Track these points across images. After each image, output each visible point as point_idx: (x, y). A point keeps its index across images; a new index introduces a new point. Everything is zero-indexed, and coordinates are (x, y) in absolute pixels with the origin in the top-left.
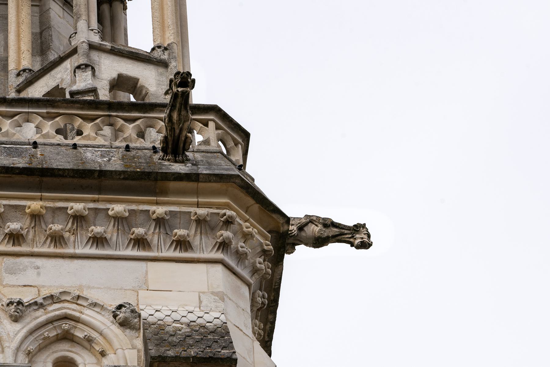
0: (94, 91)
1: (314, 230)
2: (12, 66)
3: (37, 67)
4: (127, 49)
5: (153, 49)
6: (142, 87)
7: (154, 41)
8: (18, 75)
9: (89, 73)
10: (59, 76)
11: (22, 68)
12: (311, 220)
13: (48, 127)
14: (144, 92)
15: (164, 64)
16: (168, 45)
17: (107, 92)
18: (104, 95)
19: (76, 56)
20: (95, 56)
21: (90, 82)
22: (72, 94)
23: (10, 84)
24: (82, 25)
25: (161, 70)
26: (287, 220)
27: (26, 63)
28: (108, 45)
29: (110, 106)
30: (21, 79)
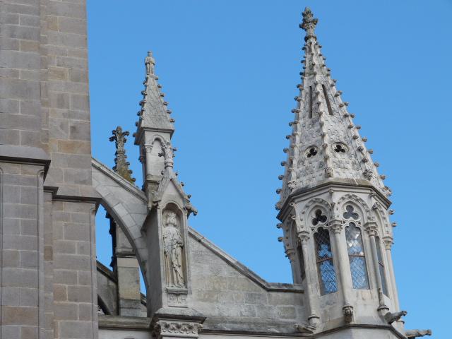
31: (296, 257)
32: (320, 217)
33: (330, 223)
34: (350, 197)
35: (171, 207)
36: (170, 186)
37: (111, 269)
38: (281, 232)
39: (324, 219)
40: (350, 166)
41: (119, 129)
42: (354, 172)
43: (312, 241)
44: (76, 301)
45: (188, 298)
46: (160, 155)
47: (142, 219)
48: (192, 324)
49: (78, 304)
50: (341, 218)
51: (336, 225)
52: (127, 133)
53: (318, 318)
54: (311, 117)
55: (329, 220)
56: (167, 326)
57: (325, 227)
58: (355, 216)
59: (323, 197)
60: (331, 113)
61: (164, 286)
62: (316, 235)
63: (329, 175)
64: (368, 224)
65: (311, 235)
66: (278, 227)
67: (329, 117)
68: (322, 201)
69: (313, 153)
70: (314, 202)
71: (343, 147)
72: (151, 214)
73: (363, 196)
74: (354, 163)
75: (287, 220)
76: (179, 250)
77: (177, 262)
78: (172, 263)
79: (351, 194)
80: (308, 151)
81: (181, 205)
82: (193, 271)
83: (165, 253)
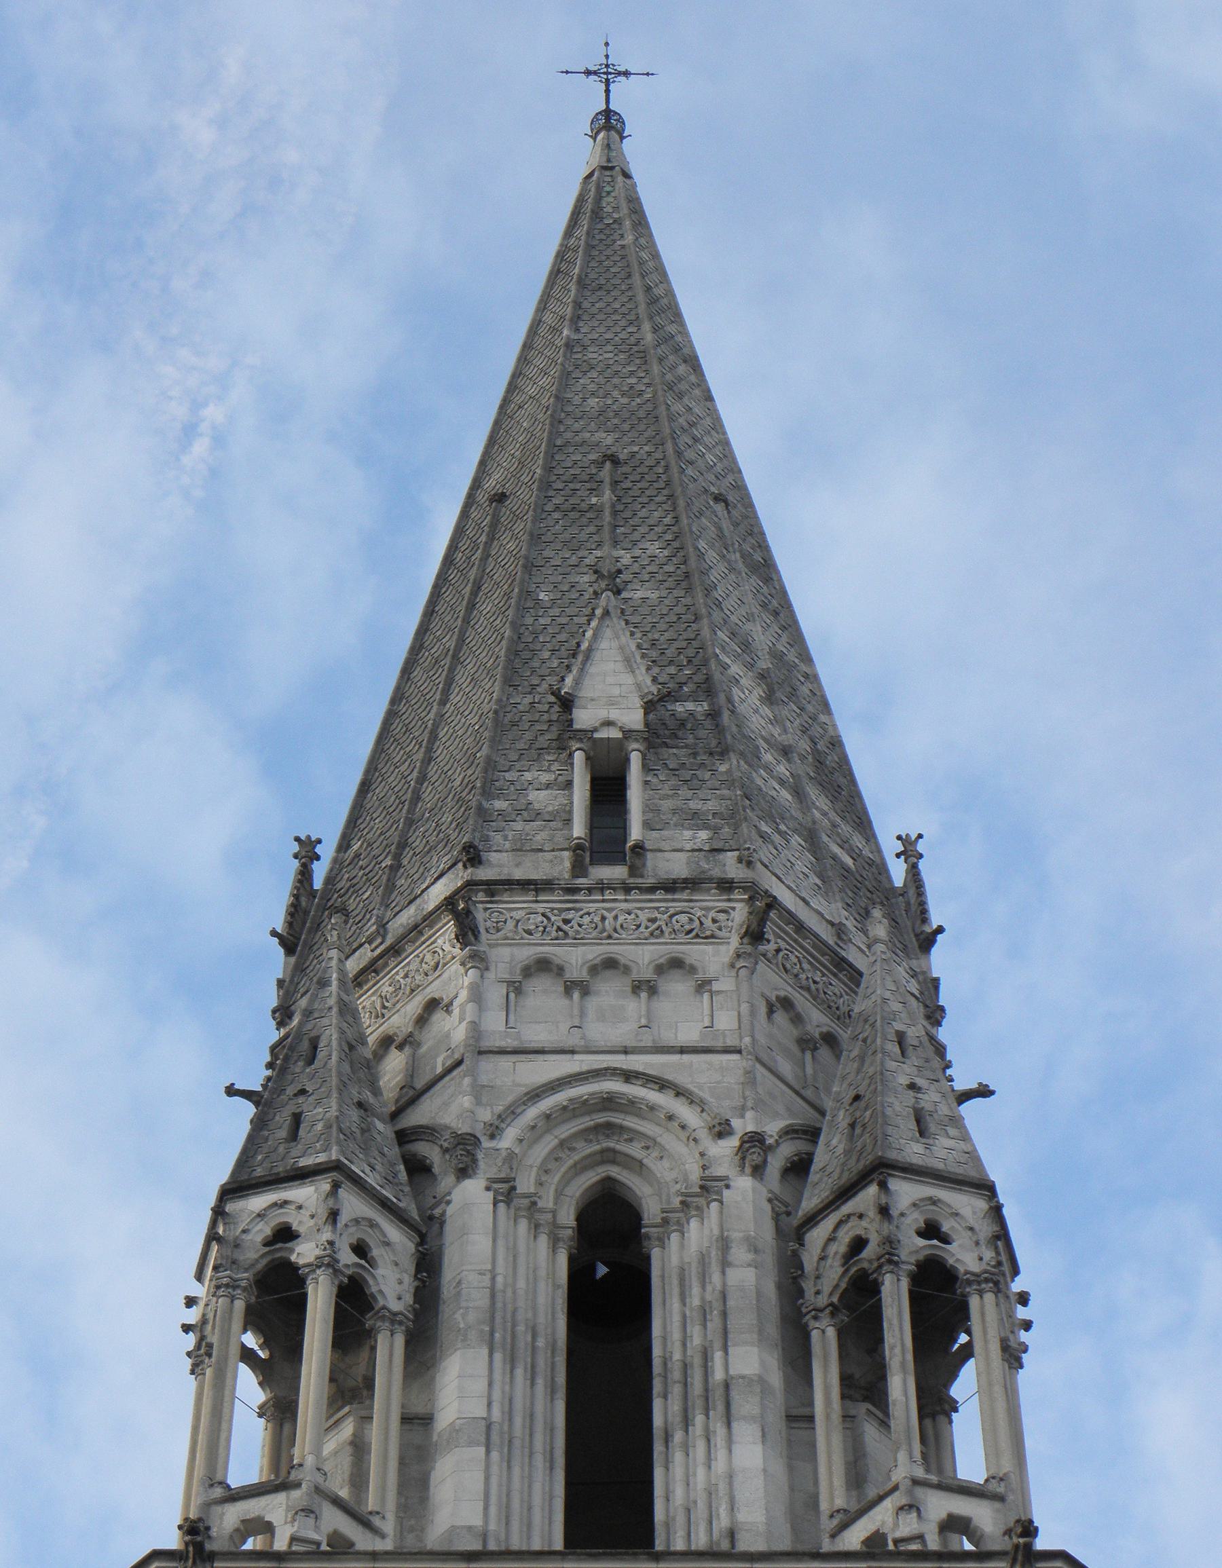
0: (920, 1537)
2: (824, 1506)
3: (854, 1507)
4: (956, 1483)
5: (987, 1481)
6: (977, 1528)
7: (987, 1470)
8: (832, 1516)
9: (915, 1514)
10: (879, 1518)
11: (836, 1508)
14: (979, 1533)
15: (1000, 1498)
16: (1005, 1474)
17: (936, 1537)
18: (933, 1544)
19: (897, 1494)
20: (920, 1492)
21: (916, 1526)
22: (896, 1542)
23: (822, 1527)
24: (902, 1456)
25: (997, 1505)
27: (840, 1502)
28: (934, 1478)
29: (940, 1556)
30: (835, 1522)
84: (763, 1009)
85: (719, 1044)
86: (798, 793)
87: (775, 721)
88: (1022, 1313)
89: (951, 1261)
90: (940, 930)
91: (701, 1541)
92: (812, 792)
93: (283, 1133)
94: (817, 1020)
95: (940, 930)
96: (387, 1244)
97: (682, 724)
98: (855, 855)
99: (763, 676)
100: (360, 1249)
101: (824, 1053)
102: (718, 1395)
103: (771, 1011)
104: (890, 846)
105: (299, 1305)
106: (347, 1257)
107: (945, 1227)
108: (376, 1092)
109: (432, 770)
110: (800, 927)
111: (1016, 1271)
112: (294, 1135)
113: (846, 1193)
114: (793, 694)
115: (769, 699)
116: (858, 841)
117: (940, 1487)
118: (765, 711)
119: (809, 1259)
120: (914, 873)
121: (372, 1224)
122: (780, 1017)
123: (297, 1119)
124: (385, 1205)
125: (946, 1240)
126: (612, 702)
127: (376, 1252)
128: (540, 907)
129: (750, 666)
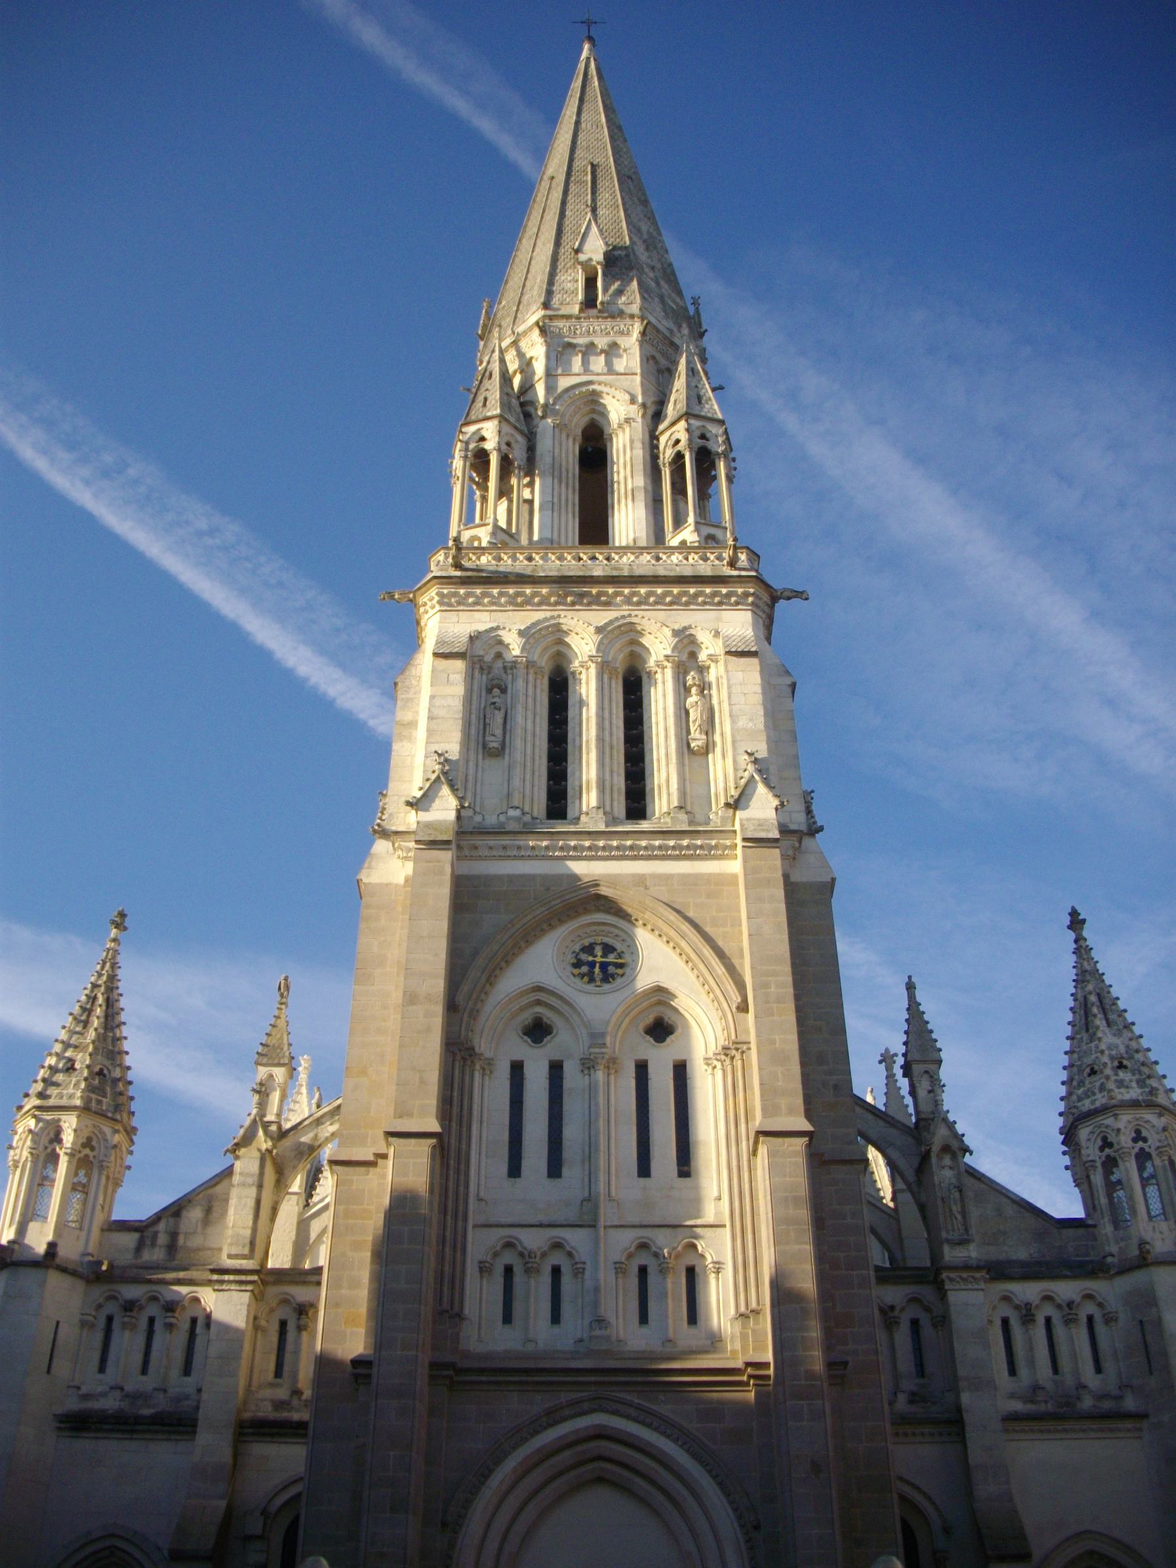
1: (787, 594)
12: (785, 590)
13: (680, 557)
26: (776, 590)
31: (1085, 1187)
32: (1106, 1144)
33: (1118, 1150)
34: (1137, 1120)
35: (946, 1149)
36: (943, 1125)
37: (891, 1205)
38: (1066, 1160)
39: (1110, 1145)
40: (1134, 1084)
41: (887, 1050)
42: (1139, 1091)
43: (1100, 1170)
44: (852, 1270)
45: (972, 1246)
46: (930, 1092)
47: (916, 1164)
48: (978, 1275)
49: (855, 1273)
50: (1130, 1144)
51: (1123, 1153)
52: (896, 1055)
53: (1113, 1256)
54: (1087, 1030)
55: (1116, 1147)
56: (951, 1280)
57: (1113, 1154)
58: (1145, 1140)
59: (1107, 1122)
60: (1109, 1024)
61: (944, 1235)
62: (1104, 1164)
63: (1112, 1098)
64: (1158, 1148)
65: (1099, 1164)
66: (1064, 1153)
67: (1107, 1030)
68: (1107, 1126)
69: (1093, 1072)
70: (1099, 1127)
71: (1125, 1062)
72: (925, 1157)
73: (1149, 1116)
74: (1138, 1082)
75: (1073, 1147)
76: (957, 1195)
77: (956, 1209)
78: (951, 1210)
79: (1138, 1116)
80: (1088, 1070)
81: (955, 1145)
82: (974, 1213)
83: (943, 1199)
84: (645, 359)
85: (630, 372)
86: (658, 284)
87: (649, 257)
88: (733, 464)
89: (709, 447)
90: (706, 331)
91: (624, 544)
92: (662, 283)
93: (481, 404)
94: (663, 362)
95: (706, 331)
96: (517, 441)
97: (617, 259)
98: (678, 305)
99: (645, 241)
100: (508, 444)
101: (666, 374)
102: (629, 493)
103: (648, 359)
104: (689, 302)
105: (488, 463)
106: (504, 447)
107: (708, 435)
108: (513, 389)
109: (530, 276)
110: (658, 331)
111: (731, 450)
112: (485, 405)
113: (673, 424)
114: (655, 248)
115: (647, 249)
116: (678, 300)
117: (704, 524)
118: (646, 254)
119: (661, 448)
120: (697, 310)
121: (512, 435)
122: (651, 362)
123: (486, 399)
124: (516, 428)
125: (707, 440)
126: (592, 251)
127: (514, 445)
128: (568, 324)
129: (640, 238)
